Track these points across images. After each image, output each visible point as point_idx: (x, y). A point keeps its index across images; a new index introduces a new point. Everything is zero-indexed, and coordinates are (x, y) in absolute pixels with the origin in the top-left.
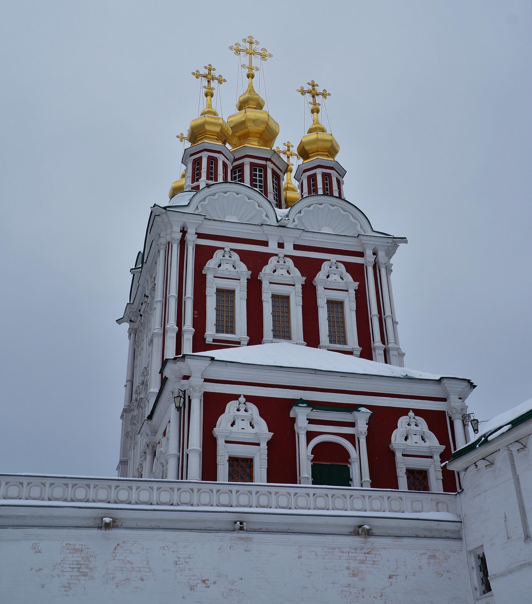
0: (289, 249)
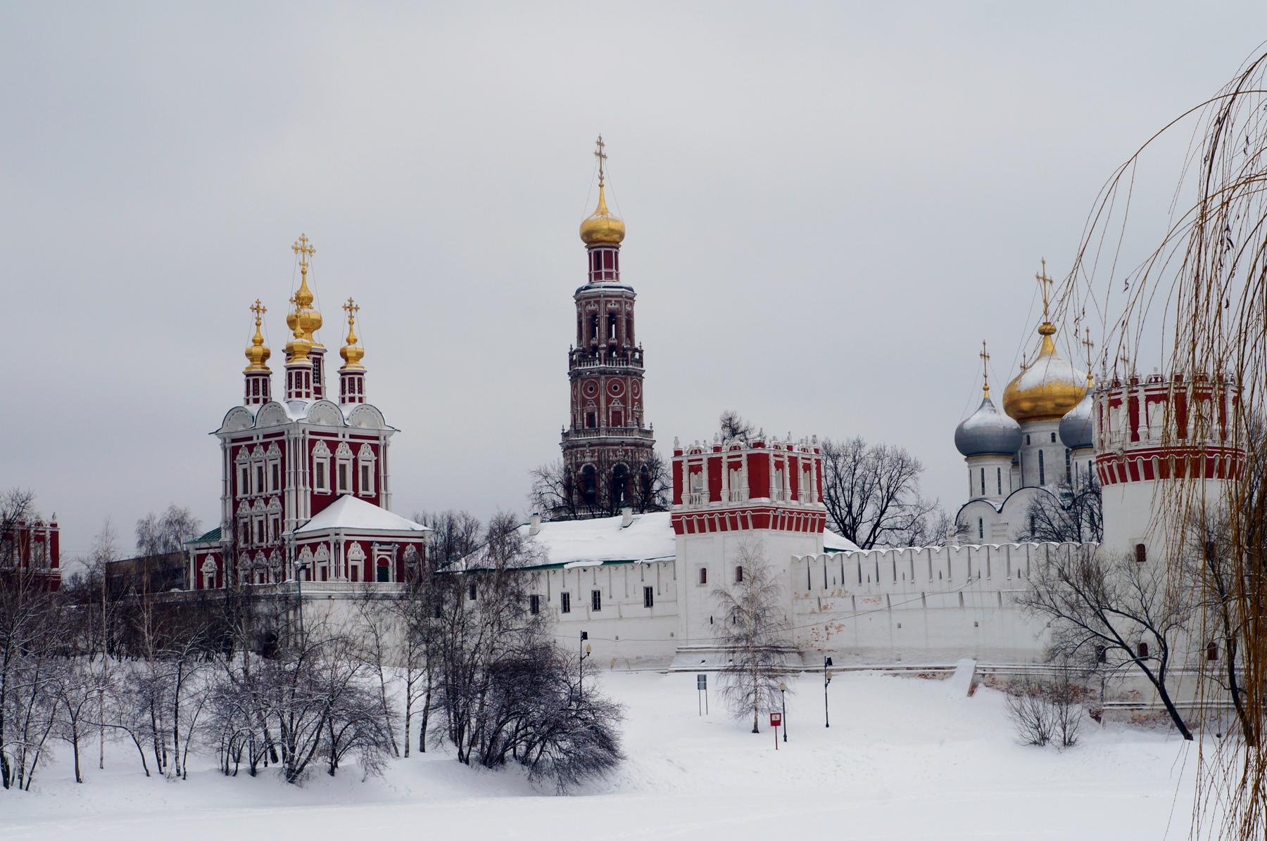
0: (347, 439)
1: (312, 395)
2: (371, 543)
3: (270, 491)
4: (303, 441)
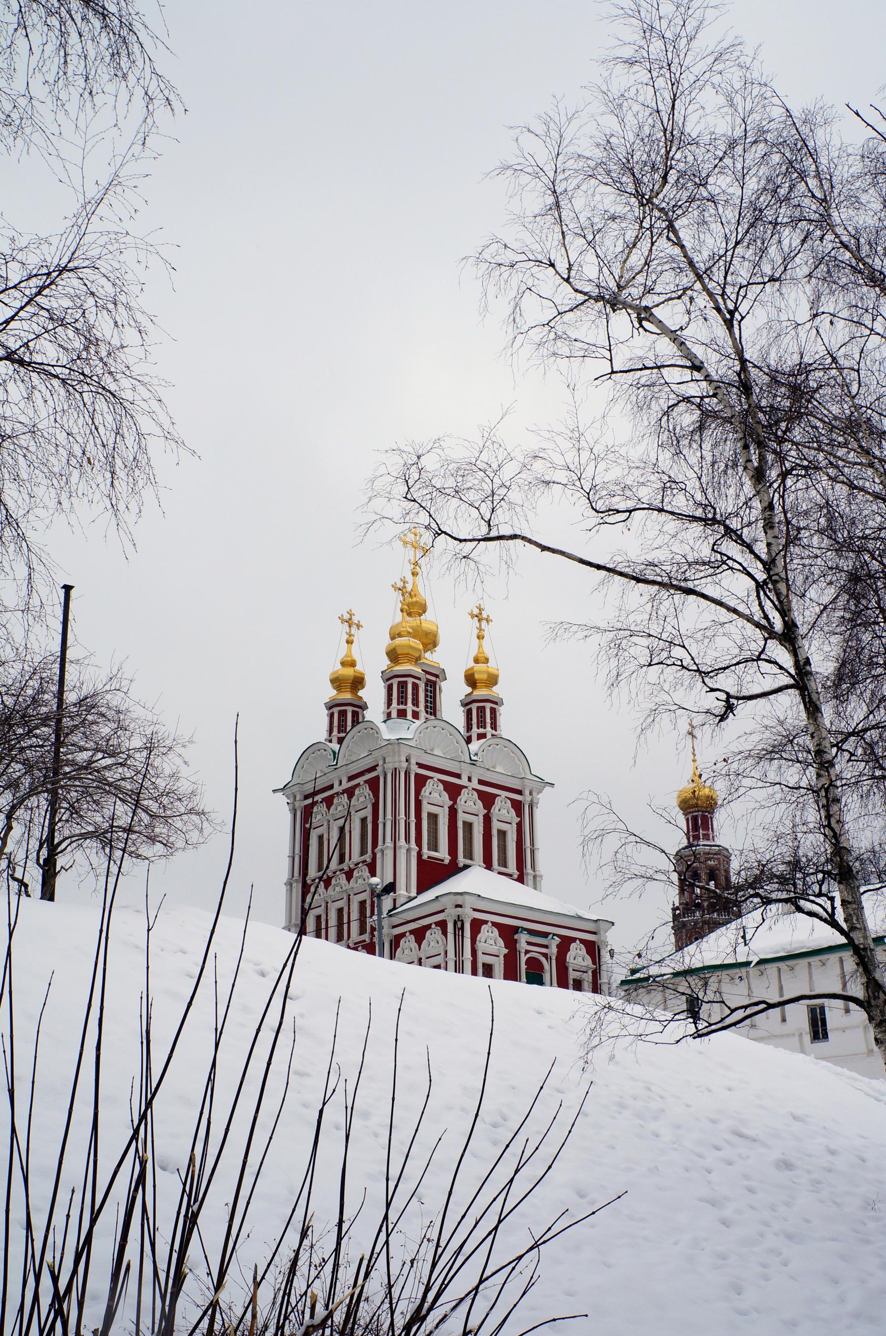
1: (423, 714)
2: (516, 930)
3: (356, 857)
4: (407, 774)
